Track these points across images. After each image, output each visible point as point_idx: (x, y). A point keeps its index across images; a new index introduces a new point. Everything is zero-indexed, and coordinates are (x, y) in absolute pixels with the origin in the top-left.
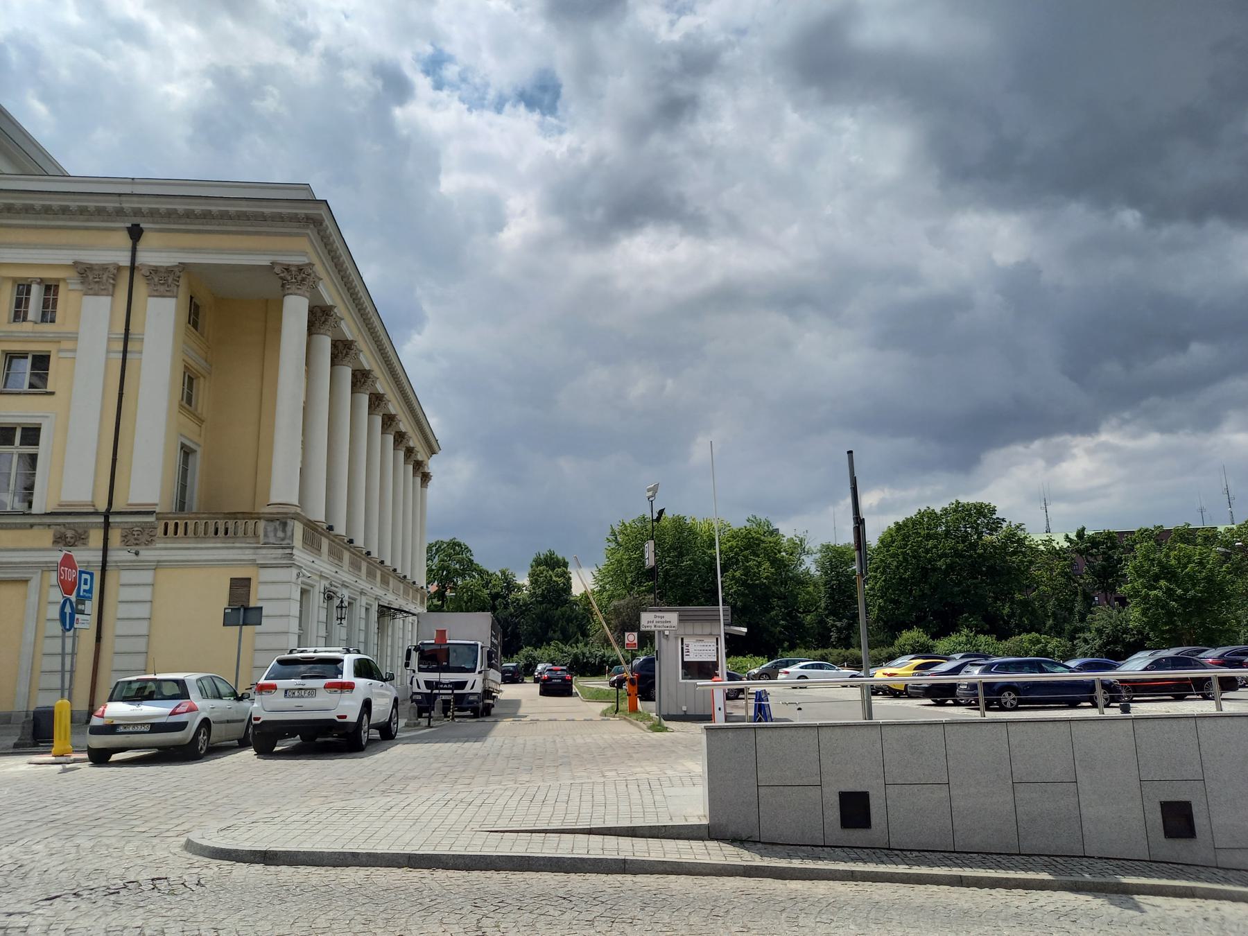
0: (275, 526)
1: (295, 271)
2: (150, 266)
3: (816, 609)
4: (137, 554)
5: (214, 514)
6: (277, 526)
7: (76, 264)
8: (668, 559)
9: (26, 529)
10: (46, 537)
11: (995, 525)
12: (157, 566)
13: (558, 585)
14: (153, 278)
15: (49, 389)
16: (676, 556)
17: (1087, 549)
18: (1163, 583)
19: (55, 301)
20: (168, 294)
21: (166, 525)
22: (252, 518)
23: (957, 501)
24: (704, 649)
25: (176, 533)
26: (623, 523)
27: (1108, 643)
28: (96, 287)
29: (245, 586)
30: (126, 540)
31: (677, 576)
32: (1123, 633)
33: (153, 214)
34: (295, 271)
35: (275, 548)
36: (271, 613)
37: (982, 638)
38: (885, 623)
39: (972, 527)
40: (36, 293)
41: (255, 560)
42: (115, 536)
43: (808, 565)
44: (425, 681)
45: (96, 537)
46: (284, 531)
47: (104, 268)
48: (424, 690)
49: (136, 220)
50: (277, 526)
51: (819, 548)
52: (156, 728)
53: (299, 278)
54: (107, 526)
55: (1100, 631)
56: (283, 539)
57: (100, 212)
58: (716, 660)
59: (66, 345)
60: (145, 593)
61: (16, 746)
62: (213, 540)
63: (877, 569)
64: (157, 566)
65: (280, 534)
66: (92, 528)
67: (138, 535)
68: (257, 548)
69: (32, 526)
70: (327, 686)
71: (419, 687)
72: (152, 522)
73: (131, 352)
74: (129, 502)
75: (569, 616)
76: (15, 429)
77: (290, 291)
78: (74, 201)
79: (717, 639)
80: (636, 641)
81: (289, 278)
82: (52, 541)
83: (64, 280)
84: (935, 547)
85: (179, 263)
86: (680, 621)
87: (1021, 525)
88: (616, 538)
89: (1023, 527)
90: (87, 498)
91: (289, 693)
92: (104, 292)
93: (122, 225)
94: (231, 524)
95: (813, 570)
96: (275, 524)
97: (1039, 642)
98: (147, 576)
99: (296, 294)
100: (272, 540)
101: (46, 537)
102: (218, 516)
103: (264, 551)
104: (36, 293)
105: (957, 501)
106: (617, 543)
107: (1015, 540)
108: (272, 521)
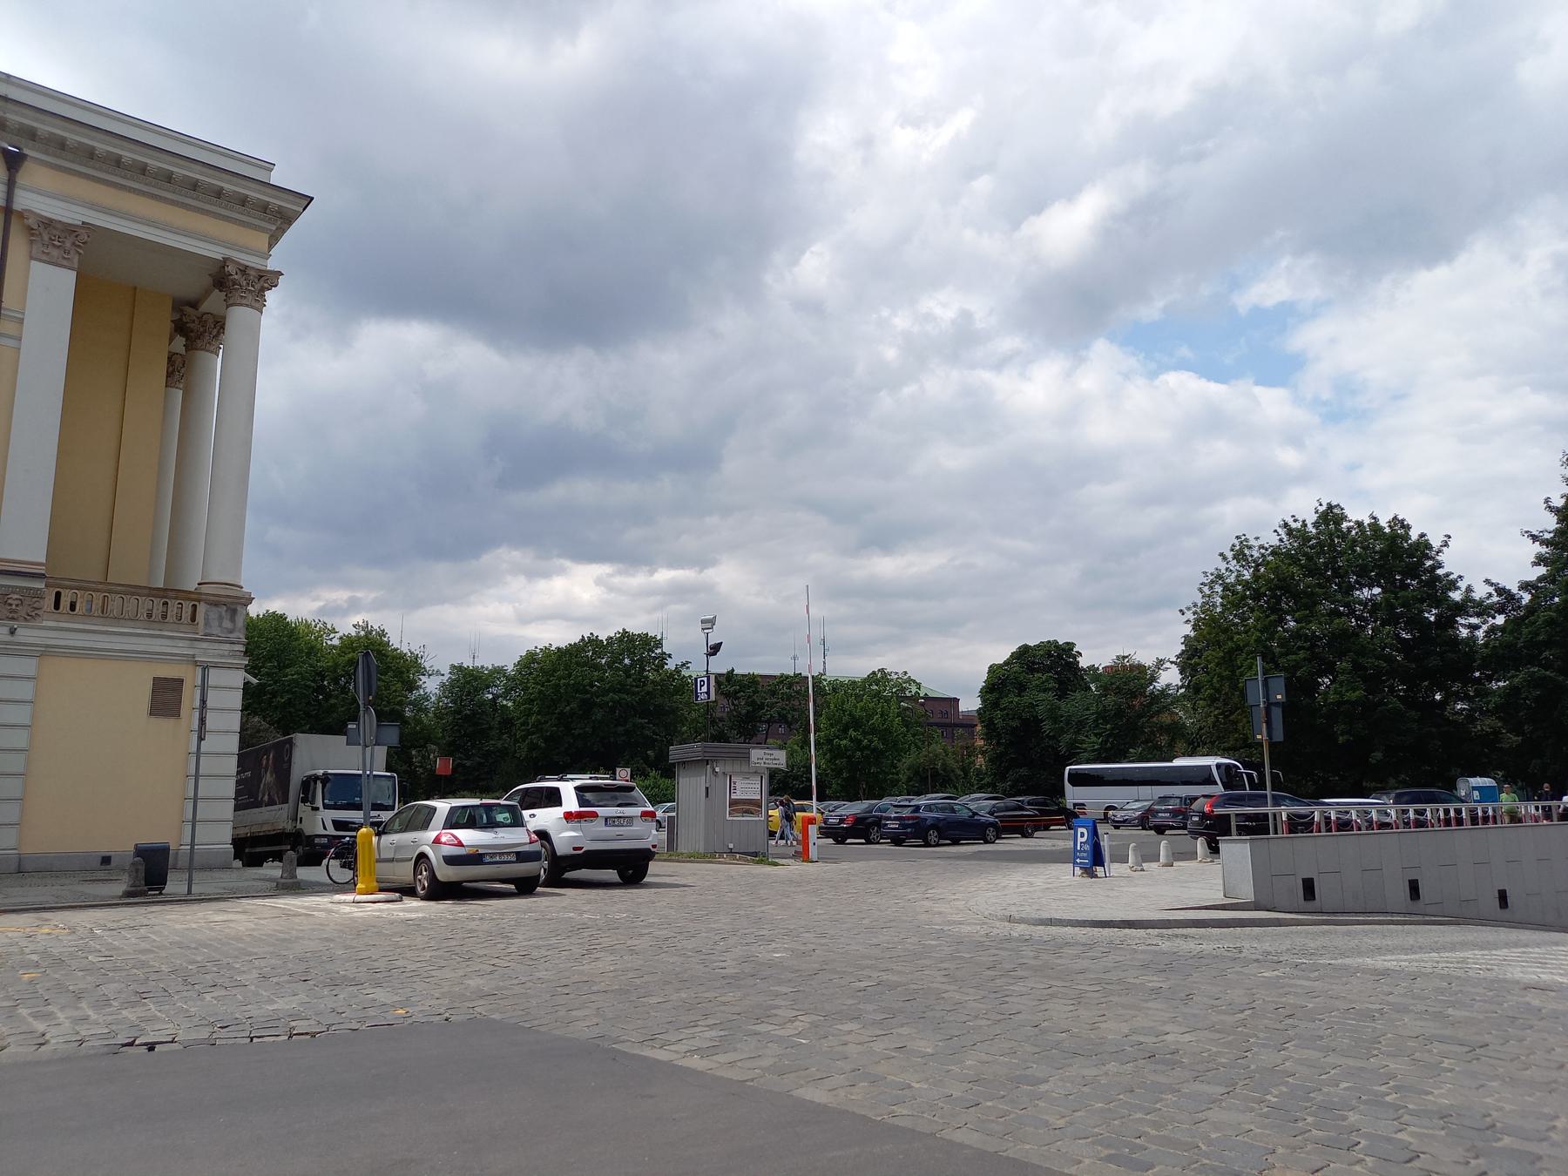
0: (221, 612)
1: (254, 277)
2: (42, 216)
4: (12, 632)
5: (136, 587)
6: (224, 613)
12: (45, 652)
14: (40, 234)
17: (736, 692)
18: (852, 732)
20: (65, 263)
21: (58, 595)
22: (86, 589)
23: (624, 630)
31: (274, 694)
32: (793, 780)
34: (254, 277)
35: (220, 642)
41: (194, 656)
44: (333, 821)
46: (233, 620)
48: (331, 831)
50: (224, 613)
53: (258, 286)
56: (231, 632)
58: (759, 798)
60: (24, 690)
61: (128, 894)
64: (45, 652)
65: (227, 624)
67: (17, 605)
68: (196, 640)
71: (325, 828)
72: (38, 589)
77: (244, 302)
78: (157, 159)
79: (762, 777)
85: (83, 223)
87: (688, 663)
89: (689, 665)
91: (609, 822)
96: (220, 610)
98: (27, 666)
99: (252, 307)
100: (216, 630)
102: (139, 591)
103: (205, 645)
105: (624, 630)
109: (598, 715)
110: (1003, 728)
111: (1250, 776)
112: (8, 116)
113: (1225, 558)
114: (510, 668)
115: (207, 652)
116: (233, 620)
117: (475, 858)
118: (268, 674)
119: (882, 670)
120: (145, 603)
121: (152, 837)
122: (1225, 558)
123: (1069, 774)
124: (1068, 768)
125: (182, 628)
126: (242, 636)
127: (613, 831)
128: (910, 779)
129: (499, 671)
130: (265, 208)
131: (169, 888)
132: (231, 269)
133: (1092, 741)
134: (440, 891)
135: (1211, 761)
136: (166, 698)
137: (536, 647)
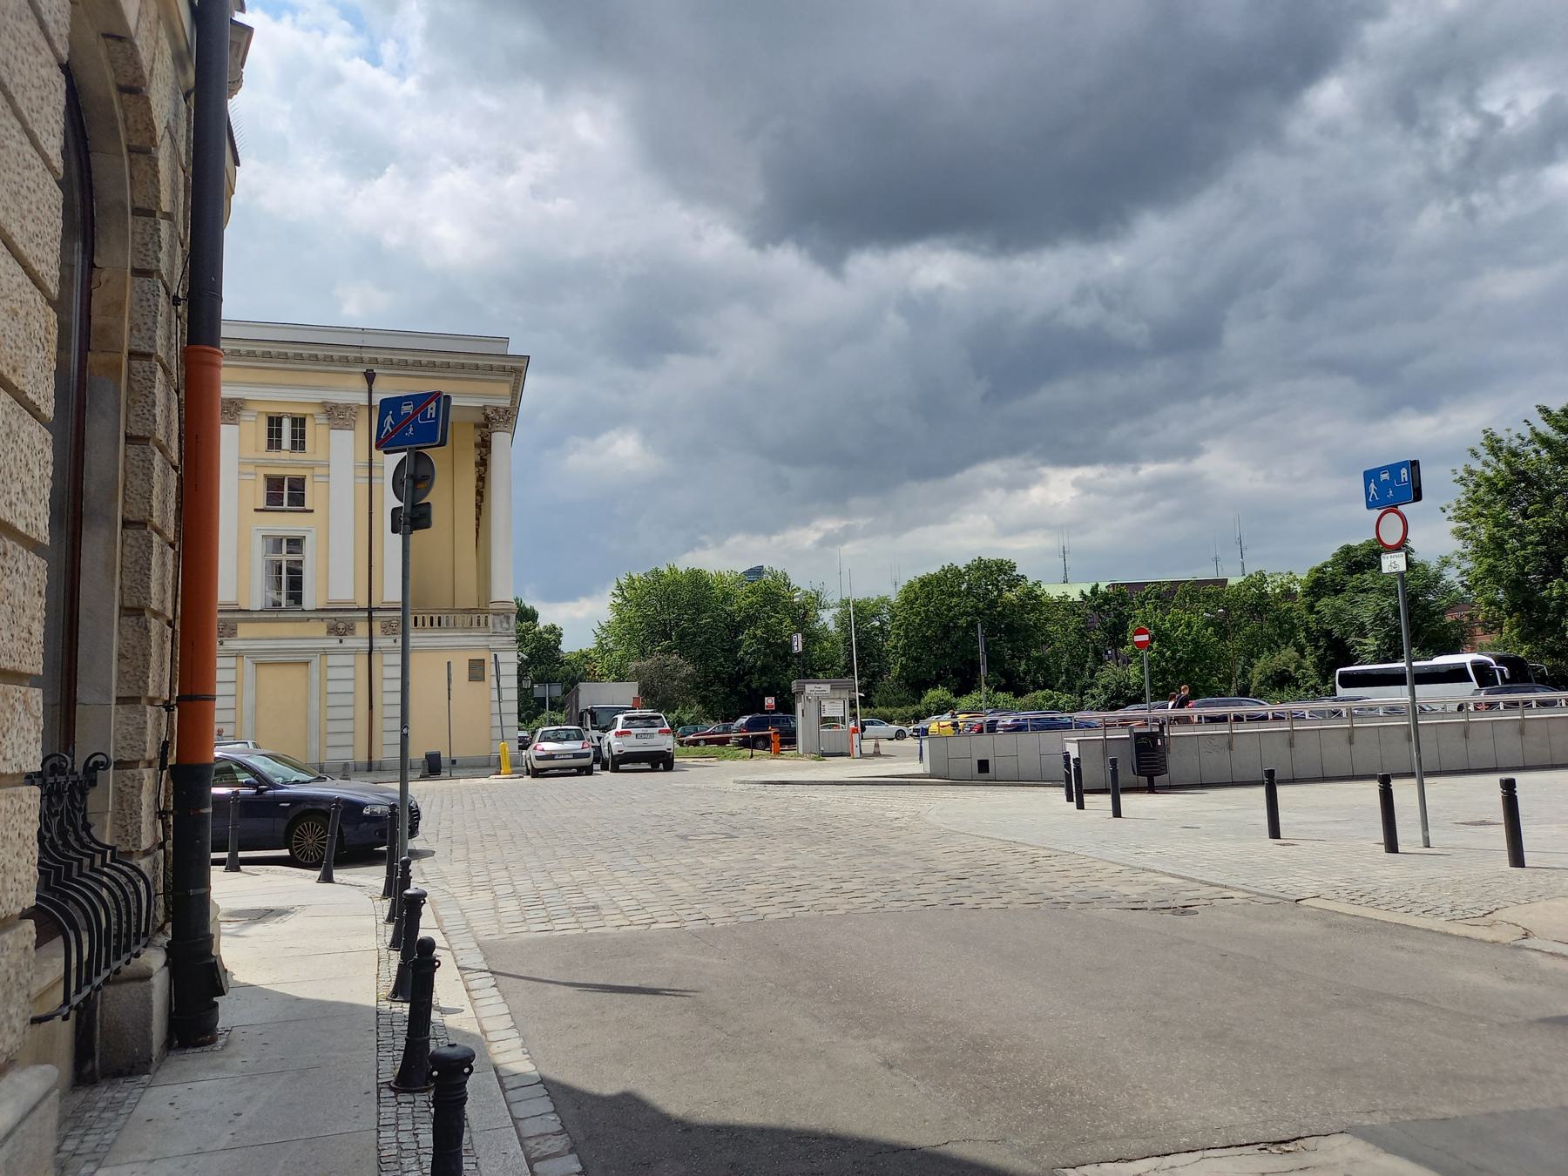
7: (323, 404)
8: (686, 616)
10: (322, 629)
11: (1014, 582)
13: (549, 642)
16: (694, 613)
17: (1099, 606)
19: (303, 435)
21: (416, 618)
23: (980, 558)
24: (835, 709)
26: (630, 576)
27: (1112, 698)
28: (341, 422)
30: (384, 630)
33: (389, 363)
36: (221, 680)
37: (1001, 695)
38: (907, 682)
39: (993, 584)
40: (286, 426)
42: (377, 626)
43: (826, 620)
45: (362, 629)
46: (508, 623)
47: (348, 407)
51: (837, 600)
52: (576, 756)
53: (506, 418)
54: (370, 619)
55: (1105, 687)
56: (507, 630)
57: (345, 361)
59: (318, 471)
63: (900, 626)
65: (505, 625)
66: (358, 621)
69: (308, 620)
70: (660, 732)
71: (593, 742)
73: (375, 478)
74: (385, 600)
75: (574, 678)
76: (282, 540)
82: (326, 631)
83: (312, 415)
84: (957, 605)
86: (831, 689)
87: (1038, 582)
92: (348, 427)
93: (360, 370)
95: (832, 627)
97: (1051, 698)
103: (493, 639)
104: (286, 426)
105: (980, 558)
106: (625, 598)
107: (1033, 600)
108: (498, 615)
109: (956, 636)
110: (1318, 631)
111: (1501, 672)
112: (363, 355)
113: (1475, 454)
114: (894, 598)
115: (496, 642)
116: (508, 623)
117: (551, 757)
118: (688, 620)
120: (467, 618)
121: (433, 749)
122: (1475, 454)
123: (1340, 676)
124: (1338, 671)
125: (480, 630)
126: (514, 631)
127: (641, 741)
128: (1261, 683)
129: (884, 601)
131: (442, 774)
132: (488, 412)
133: (1371, 643)
134: (536, 773)
135: (1466, 659)
136: (476, 670)
137: (916, 577)
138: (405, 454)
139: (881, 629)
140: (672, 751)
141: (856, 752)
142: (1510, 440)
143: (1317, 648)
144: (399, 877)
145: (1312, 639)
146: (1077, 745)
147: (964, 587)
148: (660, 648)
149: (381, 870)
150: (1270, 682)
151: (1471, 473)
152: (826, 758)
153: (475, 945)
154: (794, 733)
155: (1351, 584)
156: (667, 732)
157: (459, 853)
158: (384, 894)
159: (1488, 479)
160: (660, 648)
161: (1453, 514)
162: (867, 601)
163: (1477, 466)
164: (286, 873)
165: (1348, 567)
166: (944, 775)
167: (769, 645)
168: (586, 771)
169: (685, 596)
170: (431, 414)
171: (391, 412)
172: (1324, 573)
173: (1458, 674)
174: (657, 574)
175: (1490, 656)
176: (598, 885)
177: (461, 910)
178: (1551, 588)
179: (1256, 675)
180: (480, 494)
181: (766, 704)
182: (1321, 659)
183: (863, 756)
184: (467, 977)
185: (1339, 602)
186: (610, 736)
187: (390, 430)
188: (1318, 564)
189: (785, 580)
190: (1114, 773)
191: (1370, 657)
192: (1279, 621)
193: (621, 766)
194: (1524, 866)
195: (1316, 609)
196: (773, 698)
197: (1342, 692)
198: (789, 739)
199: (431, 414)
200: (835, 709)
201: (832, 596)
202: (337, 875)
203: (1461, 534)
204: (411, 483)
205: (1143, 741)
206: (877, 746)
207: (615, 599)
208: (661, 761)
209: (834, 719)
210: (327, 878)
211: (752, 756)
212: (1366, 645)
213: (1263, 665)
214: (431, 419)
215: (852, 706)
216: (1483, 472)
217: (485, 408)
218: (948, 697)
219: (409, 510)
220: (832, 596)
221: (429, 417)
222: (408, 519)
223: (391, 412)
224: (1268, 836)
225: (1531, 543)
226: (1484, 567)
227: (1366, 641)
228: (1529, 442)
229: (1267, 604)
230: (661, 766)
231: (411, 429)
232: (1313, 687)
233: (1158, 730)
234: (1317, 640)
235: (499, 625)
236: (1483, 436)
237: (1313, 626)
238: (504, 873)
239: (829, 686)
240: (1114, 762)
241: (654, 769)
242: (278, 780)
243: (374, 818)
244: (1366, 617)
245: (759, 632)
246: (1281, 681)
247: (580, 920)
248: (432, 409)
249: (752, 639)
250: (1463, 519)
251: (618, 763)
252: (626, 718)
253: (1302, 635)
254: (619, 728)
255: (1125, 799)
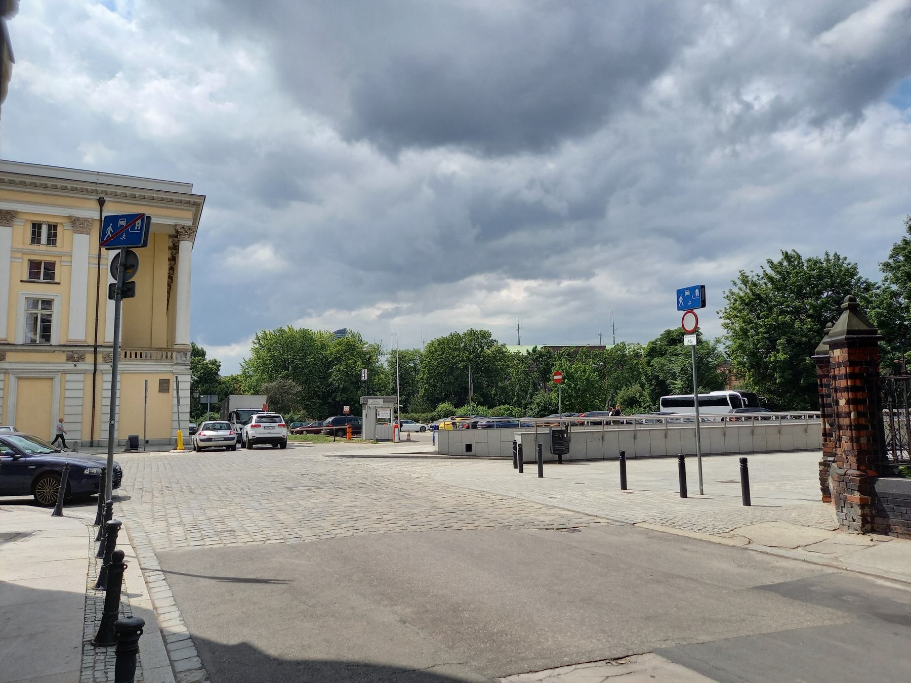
3: (385, 389)
7: (70, 217)
9: (51, 352)
10: (63, 357)
11: (491, 344)
13: (213, 370)
15: (56, 280)
16: (303, 356)
17: (537, 358)
19: (55, 235)
21: (126, 353)
23: (471, 329)
24: (385, 414)
25: (131, 357)
26: (265, 332)
27: (542, 411)
29: (167, 383)
33: (115, 194)
37: (480, 408)
38: (428, 398)
40: (44, 230)
42: (100, 358)
43: (382, 362)
45: (90, 358)
46: (186, 357)
47: (86, 220)
49: (102, 196)
51: (390, 351)
52: (226, 439)
53: (189, 232)
54: (95, 352)
55: (538, 404)
56: (185, 361)
57: (86, 191)
59: (64, 259)
62: (150, 361)
63: (426, 367)
65: (184, 359)
66: (87, 353)
69: (54, 351)
70: (279, 425)
71: (237, 431)
73: (102, 265)
74: (105, 341)
75: (227, 392)
76: (38, 301)
77: (184, 239)
80: (349, 410)
81: (184, 232)
82: (66, 358)
83: (62, 224)
84: (458, 355)
86: (384, 402)
87: (504, 344)
88: (259, 341)
90: (82, 338)
92: (85, 232)
93: (95, 198)
94: (149, 353)
95: (386, 365)
99: (187, 241)
100: (180, 361)
101: (63, 357)
104: (44, 230)
105: (471, 329)
106: (261, 345)
107: (501, 354)
111: (744, 400)
113: (735, 284)
114: (422, 350)
115: (177, 369)
116: (186, 357)
117: (209, 439)
118: (299, 359)
119: (623, 343)
120: (159, 353)
121: (134, 434)
122: (735, 284)
124: (661, 398)
125: (168, 361)
126: (189, 363)
129: (417, 352)
130: (189, 203)
132: (178, 228)
133: (679, 383)
134: (200, 449)
135: (726, 393)
136: (164, 386)
138: (120, 251)
139: (414, 368)
140: (286, 437)
141: (397, 439)
142: (753, 277)
143: (651, 385)
144: (105, 513)
145: (649, 380)
146: (520, 436)
147: (463, 345)
148: (281, 375)
149: (95, 508)
150: (626, 403)
151: (732, 293)
152: (380, 442)
153: (153, 554)
154: (360, 427)
155: (669, 351)
156: (283, 426)
157: (147, 497)
158: (95, 523)
159: (741, 298)
160: (281, 375)
161: (722, 315)
162: (407, 352)
163: (736, 290)
164: (30, 510)
165: (669, 342)
166: (446, 453)
167: (348, 375)
168: (232, 448)
169: (298, 345)
170: (138, 227)
171: (111, 225)
172: (656, 344)
173: (721, 402)
174: (281, 331)
175: (738, 392)
176: (235, 517)
177: (146, 533)
178: (770, 356)
179: (619, 399)
180: (171, 278)
181: (344, 410)
182: (653, 391)
183: (400, 441)
184: (146, 574)
185: (663, 360)
186: (248, 427)
187: (111, 236)
188: (653, 340)
189: (359, 337)
190: (540, 452)
191: (678, 391)
192: (632, 370)
193: (254, 446)
194: (750, 505)
195: (651, 364)
196: (349, 407)
197: (662, 409)
198: (357, 431)
199: (138, 227)
200: (385, 414)
201: (387, 348)
202: (66, 511)
203: (726, 326)
204: (123, 269)
205: (556, 435)
206: (409, 435)
207: (255, 345)
208: (279, 443)
209: (384, 420)
210: (58, 513)
211: (334, 441)
212: (675, 384)
213: (622, 394)
214: (138, 230)
215: (396, 412)
216: (738, 293)
217: (176, 226)
218: (451, 408)
219: (121, 286)
220: (387, 348)
221: (136, 229)
222: (120, 291)
223: (111, 225)
224: (620, 488)
225: (761, 332)
226: (737, 344)
227: (676, 382)
228: (762, 278)
229: (626, 360)
230: (279, 446)
231: (124, 235)
232: (648, 406)
233: (564, 428)
234: (651, 380)
235: (179, 359)
236: (739, 274)
237: (649, 373)
238: (175, 510)
239: (382, 400)
240: (540, 447)
241: (275, 447)
242: (28, 452)
243: (92, 476)
244: (677, 369)
245: (342, 368)
246: (632, 403)
247: (222, 538)
248: (138, 224)
249: (338, 371)
250: (728, 318)
251: (252, 444)
252: (259, 417)
253: (644, 378)
254: (253, 423)
255: (546, 468)
